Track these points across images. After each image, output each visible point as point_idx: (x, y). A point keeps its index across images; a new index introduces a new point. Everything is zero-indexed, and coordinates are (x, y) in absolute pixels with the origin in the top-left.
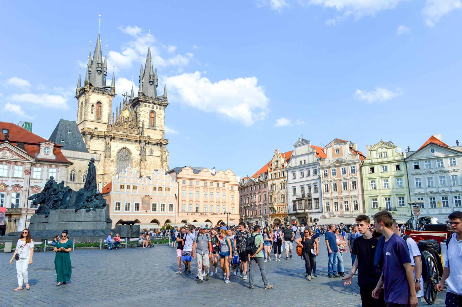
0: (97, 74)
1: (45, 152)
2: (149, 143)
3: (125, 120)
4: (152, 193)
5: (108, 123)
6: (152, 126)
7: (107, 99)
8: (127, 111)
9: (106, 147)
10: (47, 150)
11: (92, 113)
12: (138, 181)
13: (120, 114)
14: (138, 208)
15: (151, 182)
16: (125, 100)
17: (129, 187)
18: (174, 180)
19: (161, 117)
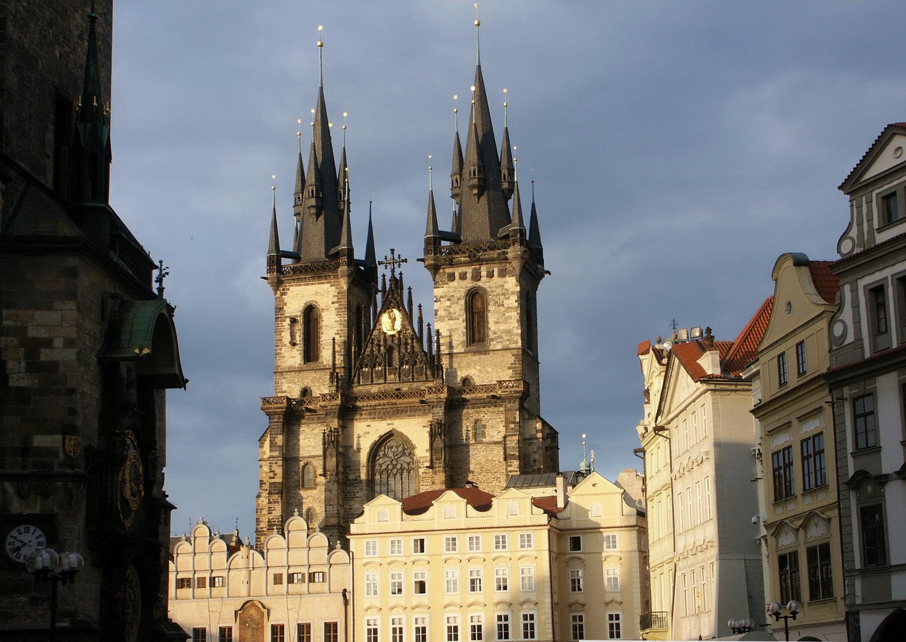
5: (334, 364)
8: (396, 312)
9: (324, 444)
16: (388, 278)
17: (201, 583)
18: (338, 546)
19: (506, 302)
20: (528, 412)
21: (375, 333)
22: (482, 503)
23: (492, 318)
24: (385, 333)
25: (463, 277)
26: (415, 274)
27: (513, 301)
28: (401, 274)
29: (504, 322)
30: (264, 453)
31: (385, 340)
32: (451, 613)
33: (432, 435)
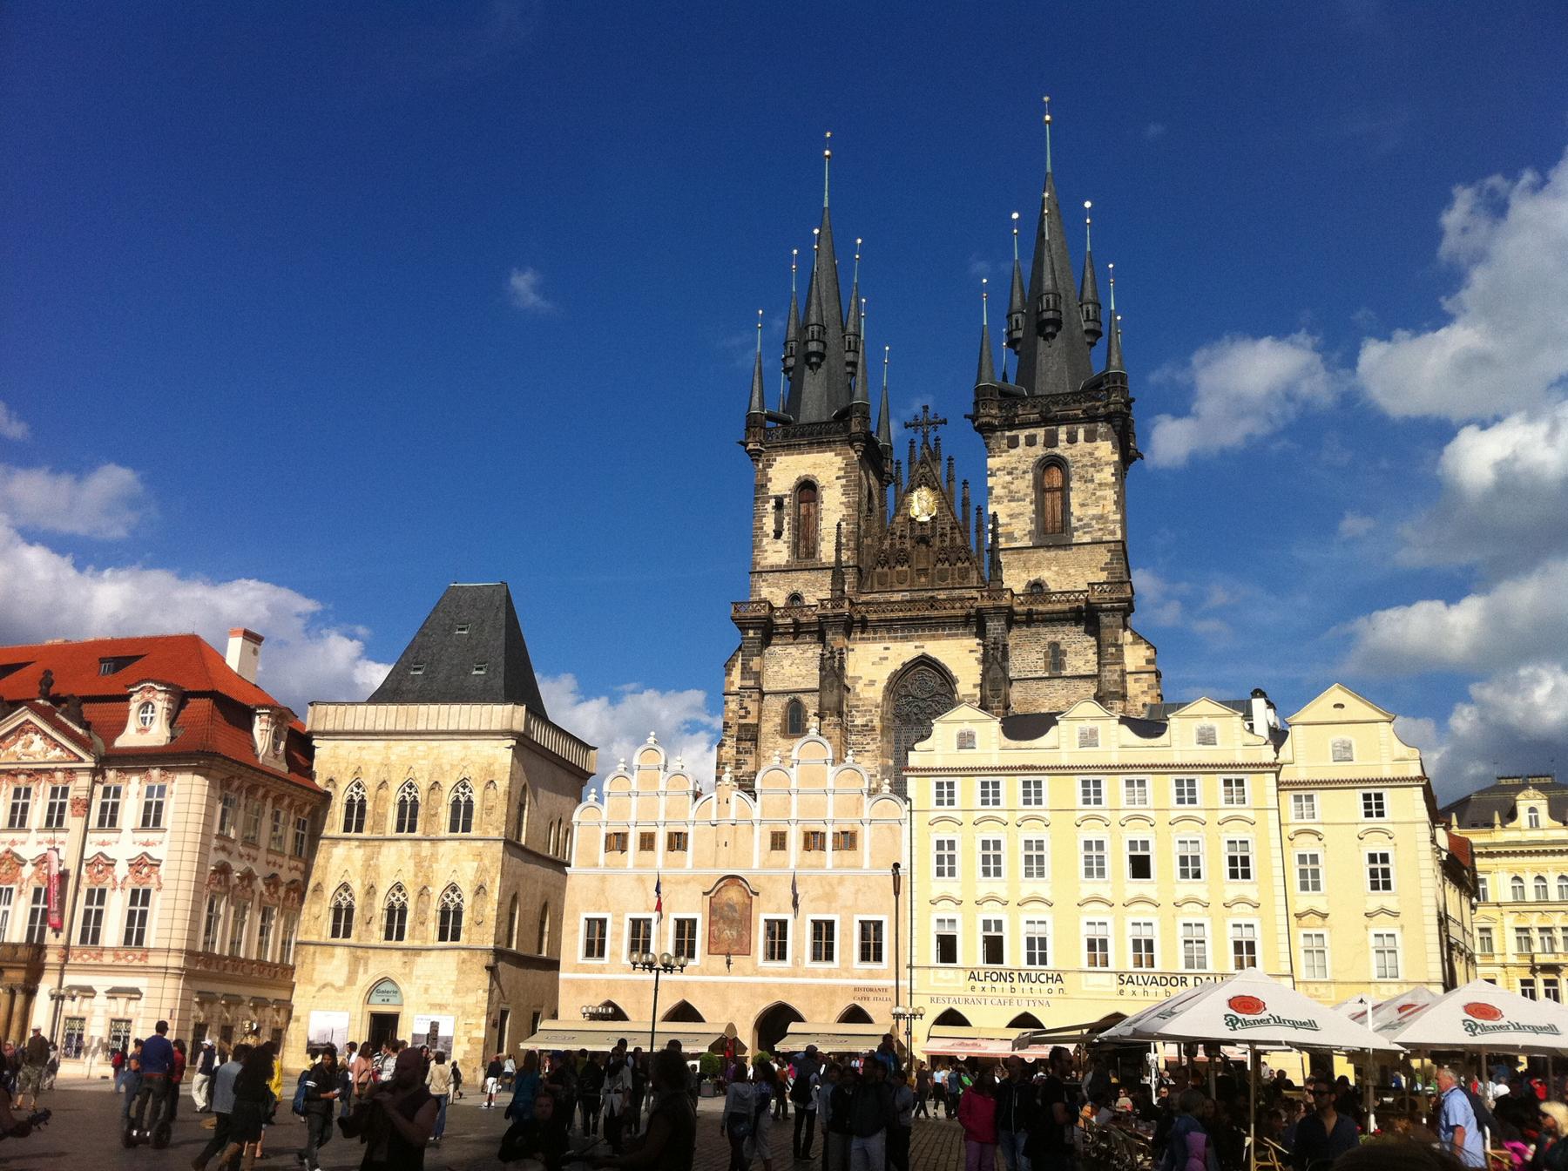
0: (808, 372)
1: (144, 720)
2: (1030, 619)
3: (918, 532)
4: (763, 866)
5: (838, 559)
6: (1054, 532)
7: (839, 461)
10: (149, 715)
11: (778, 535)
12: (692, 810)
13: (897, 510)
14: (692, 945)
15: (756, 810)
17: (647, 842)
18: (886, 788)
20: (1134, 633)
21: (899, 519)
22: (1150, 726)
23: (1075, 500)
24: (912, 520)
25: (1031, 441)
26: (956, 437)
27: (1107, 475)
28: (937, 439)
29: (1095, 501)
30: (732, 683)
31: (912, 530)
32: (1097, 912)
33: (984, 660)
